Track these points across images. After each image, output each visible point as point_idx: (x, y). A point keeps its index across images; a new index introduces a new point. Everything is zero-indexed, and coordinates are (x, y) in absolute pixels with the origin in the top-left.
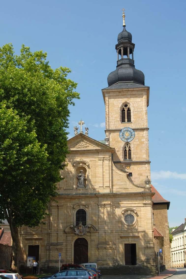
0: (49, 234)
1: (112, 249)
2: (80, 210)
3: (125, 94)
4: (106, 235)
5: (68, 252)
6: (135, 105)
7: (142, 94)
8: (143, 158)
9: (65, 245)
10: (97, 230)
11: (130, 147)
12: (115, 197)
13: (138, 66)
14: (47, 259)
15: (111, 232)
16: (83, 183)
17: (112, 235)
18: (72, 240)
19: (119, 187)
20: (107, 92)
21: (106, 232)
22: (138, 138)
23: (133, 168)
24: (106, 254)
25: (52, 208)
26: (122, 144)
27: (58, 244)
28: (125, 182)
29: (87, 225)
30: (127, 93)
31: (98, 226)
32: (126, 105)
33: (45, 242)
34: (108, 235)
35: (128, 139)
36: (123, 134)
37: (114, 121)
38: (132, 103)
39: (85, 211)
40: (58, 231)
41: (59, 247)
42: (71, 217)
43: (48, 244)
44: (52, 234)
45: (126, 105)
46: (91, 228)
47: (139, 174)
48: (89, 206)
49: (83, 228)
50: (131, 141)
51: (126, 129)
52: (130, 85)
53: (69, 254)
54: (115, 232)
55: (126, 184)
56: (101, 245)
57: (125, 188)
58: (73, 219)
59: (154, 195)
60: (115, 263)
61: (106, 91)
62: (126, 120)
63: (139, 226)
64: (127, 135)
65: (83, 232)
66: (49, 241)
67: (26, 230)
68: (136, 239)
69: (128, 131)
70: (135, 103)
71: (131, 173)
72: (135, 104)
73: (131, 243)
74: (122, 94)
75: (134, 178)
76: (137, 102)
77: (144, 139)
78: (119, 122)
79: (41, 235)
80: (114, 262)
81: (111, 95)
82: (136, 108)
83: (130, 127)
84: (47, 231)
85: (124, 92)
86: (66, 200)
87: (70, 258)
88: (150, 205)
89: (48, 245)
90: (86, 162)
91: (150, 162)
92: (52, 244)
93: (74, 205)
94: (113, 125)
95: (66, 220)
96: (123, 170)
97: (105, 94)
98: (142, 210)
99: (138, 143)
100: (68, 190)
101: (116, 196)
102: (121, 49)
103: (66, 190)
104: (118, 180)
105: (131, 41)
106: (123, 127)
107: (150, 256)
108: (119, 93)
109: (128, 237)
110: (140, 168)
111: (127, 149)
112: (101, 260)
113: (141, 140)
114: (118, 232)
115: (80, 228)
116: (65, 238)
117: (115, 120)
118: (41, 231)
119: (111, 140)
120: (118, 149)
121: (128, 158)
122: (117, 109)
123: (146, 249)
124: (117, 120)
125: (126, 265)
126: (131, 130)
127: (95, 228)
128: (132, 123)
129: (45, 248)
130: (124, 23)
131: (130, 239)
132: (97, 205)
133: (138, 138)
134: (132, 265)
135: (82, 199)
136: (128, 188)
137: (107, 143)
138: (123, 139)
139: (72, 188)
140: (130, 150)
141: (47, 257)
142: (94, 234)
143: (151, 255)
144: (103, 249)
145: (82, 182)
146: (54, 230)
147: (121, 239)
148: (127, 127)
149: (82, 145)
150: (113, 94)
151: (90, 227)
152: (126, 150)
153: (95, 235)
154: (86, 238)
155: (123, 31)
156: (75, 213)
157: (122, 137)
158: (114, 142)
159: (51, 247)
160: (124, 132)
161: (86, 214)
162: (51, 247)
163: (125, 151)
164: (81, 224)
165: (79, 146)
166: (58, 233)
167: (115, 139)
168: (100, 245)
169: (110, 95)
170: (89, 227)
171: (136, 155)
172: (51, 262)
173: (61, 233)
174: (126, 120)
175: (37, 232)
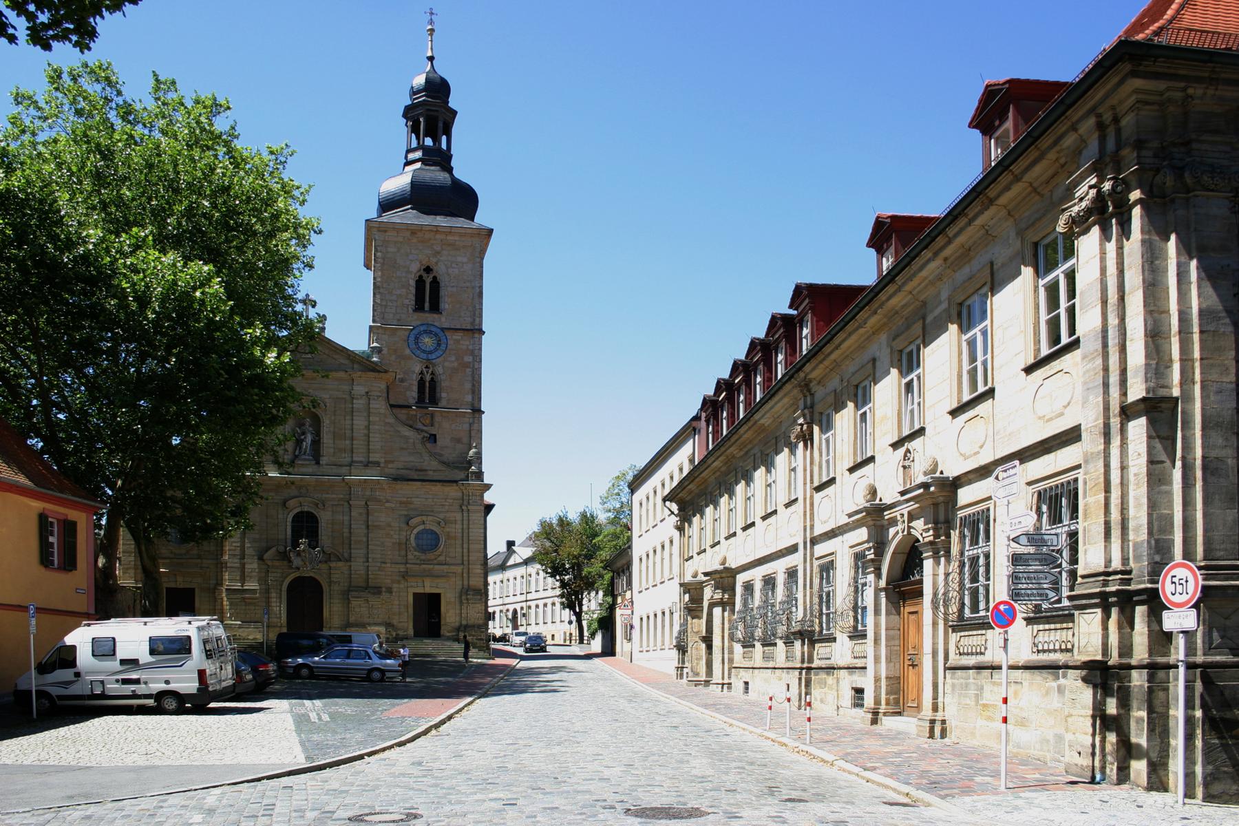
2: (302, 512)
11: (432, 373)
17: (383, 573)
35: (431, 352)
38: (446, 265)
48: (327, 506)
62: (427, 305)
69: (431, 332)
70: (454, 265)
71: (435, 435)
72: (454, 268)
77: (471, 357)
83: (435, 324)
91: (484, 412)
94: (391, 315)
99: (456, 364)
105: (448, 102)
106: (419, 323)
117: (396, 301)
120: (401, 376)
126: (438, 331)
132: (346, 504)
136: (426, 470)
154: (316, 577)
158: (393, 358)
161: (317, 522)
174: (427, 305)
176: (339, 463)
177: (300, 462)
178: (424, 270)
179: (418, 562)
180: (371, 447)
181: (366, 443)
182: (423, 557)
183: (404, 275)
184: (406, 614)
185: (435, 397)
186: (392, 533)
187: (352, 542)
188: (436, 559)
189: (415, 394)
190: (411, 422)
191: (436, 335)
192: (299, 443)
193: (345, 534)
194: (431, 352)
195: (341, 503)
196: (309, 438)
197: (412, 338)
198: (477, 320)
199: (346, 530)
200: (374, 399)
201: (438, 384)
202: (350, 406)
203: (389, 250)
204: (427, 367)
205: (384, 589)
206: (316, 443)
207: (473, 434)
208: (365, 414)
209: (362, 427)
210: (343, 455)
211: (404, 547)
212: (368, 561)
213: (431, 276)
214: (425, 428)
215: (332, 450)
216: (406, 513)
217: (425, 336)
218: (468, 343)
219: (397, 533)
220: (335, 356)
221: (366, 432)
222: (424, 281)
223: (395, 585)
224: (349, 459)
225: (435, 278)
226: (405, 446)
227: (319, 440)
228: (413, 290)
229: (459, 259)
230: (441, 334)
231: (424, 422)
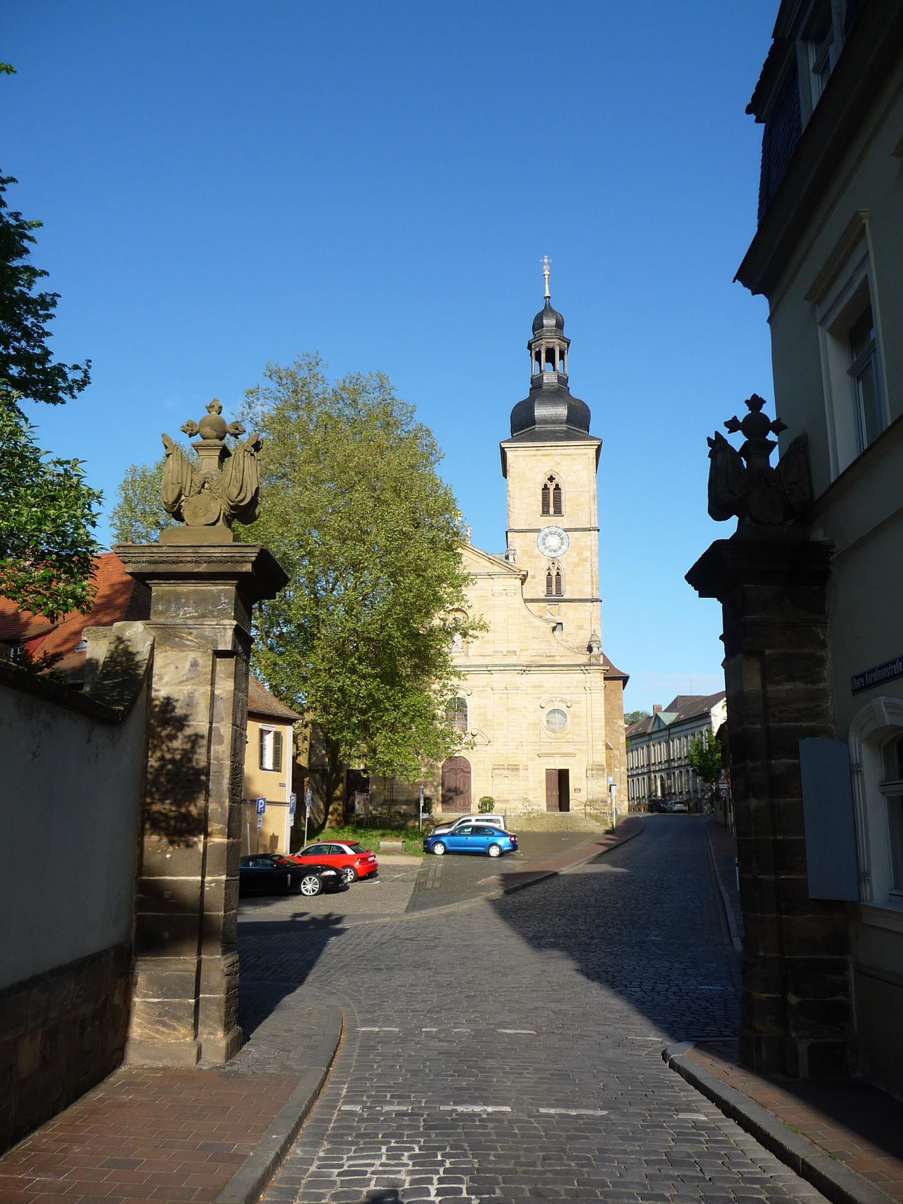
11: (558, 569)
13: (576, 391)
23: (565, 614)
26: (545, 564)
30: (554, 452)
32: (551, 476)
45: (551, 476)
48: (474, 692)
71: (561, 624)
104: (534, 638)
111: (554, 573)
121: (554, 593)
130: (547, 291)
134: (560, 811)
138: (547, 552)
140: (558, 574)
152: (549, 574)
157: (543, 547)
160: (546, 535)
168: (496, 771)
169: (517, 453)
178: (548, 479)
179: (550, 740)
182: (553, 735)
185: (560, 589)
189: (545, 588)
190: (541, 614)
201: (562, 578)
204: (553, 564)
205: (521, 767)
214: (553, 618)
216: (539, 696)
218: (586, 540)
220: (480, 560)
223: (530, 763)
225: (557, 485)
230: (564, 534)
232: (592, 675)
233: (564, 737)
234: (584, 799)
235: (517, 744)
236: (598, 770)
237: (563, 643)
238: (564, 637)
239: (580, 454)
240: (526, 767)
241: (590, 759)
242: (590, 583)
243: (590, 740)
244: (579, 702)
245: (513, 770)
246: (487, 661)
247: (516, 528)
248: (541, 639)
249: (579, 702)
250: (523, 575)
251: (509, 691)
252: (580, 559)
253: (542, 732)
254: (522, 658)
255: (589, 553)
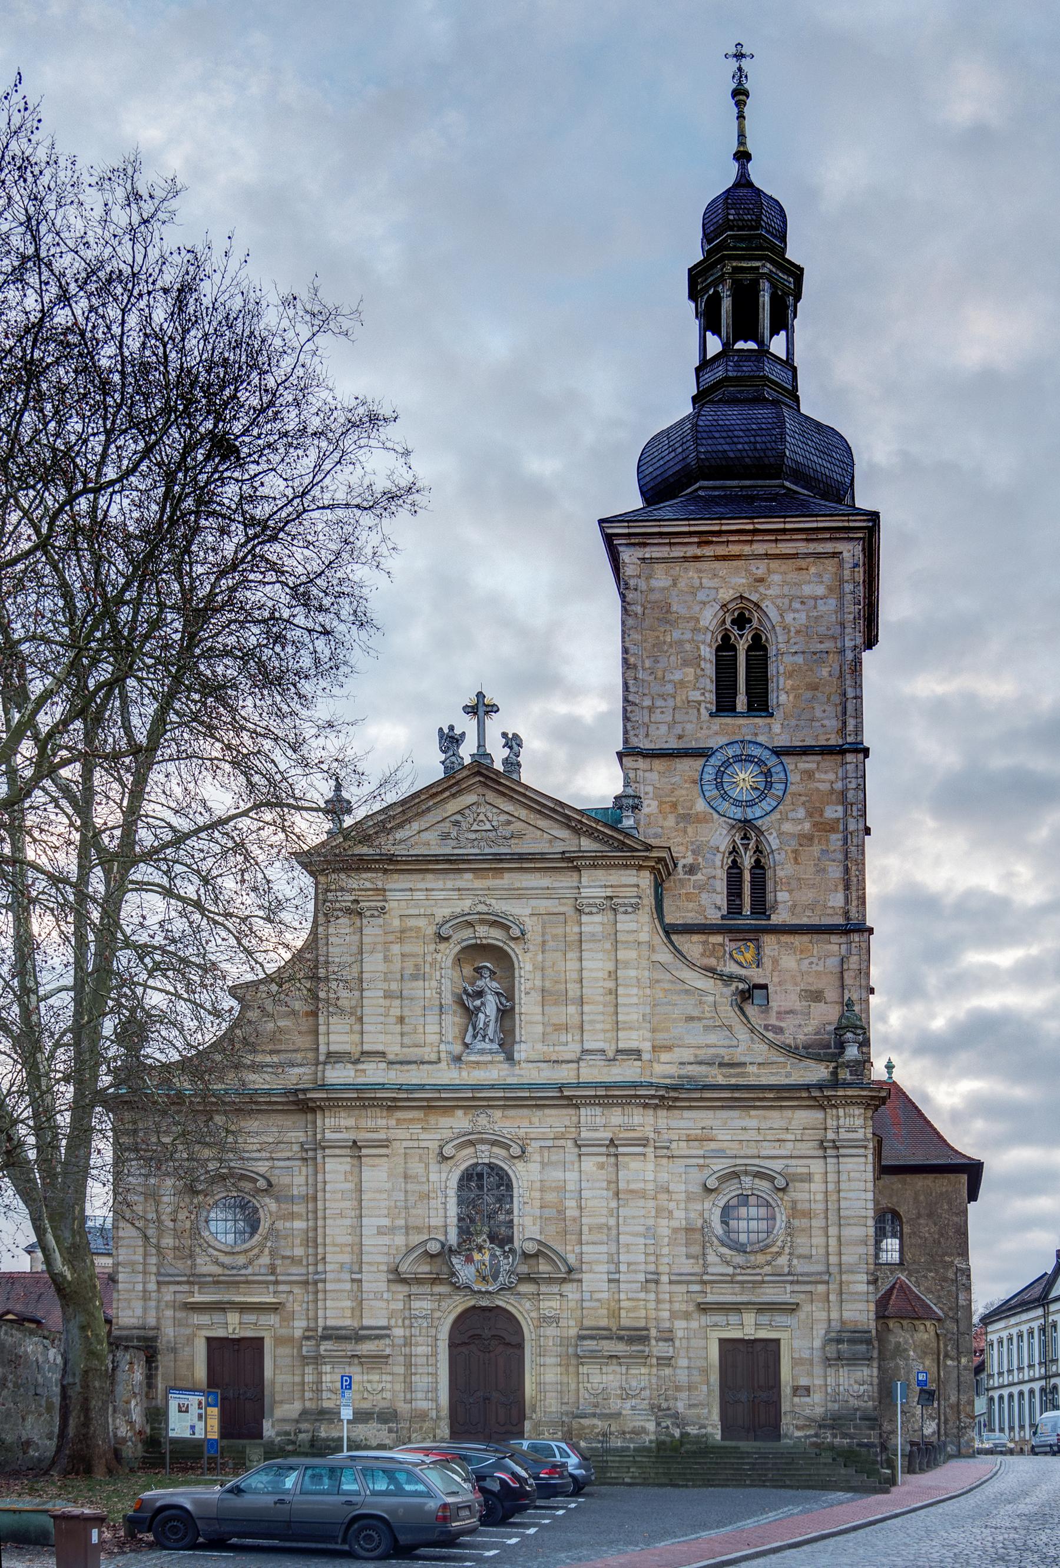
0: (316, 1283)
1: (654, 1361)
3: (734, 549)
4: (623, 1296)
5: (420, 1371)
6: (792, 615)
7: (835, 555)
8: (833, 907)
9: (401, 1341)
10: (570, 1271)
12: (670, 1108)
14: (308, 1404)
15: (647, 1281)
16: (495, 1031)
18: (437, 1314)
19: (696, 1056)
20: (629, 535)
21: (618, 1281)
22: (804, 798)
23: (775, 962)
24: (622, 1388)
25: (324, 1157)
27: (362, 1332)
28: (729, 1028)
29: (516, 1244)
30: (747, 549)
31: (577, 1249)
33: (297, 1324)
34: (630, 1295)
35: (751, 803)
36: (720, 774)
37: (671, 703)
39: (507, 1175)
40: (360, 1272)
41: (367, 1348)
42: (433, 1202)
43: (311, 1334)
44: (329, 1286)
45: (741, 615)
46: (541, 1260)
47: (806, 991)
48: (529, 1149)
49: (493, 1256)
50: (767, 818)
51: (735, 750)
52: (766, 500)
53: (421, 1381)
54: (671, 1282)
55: (735, 1043)
56: (595, 1343)
57: (726, 1060)
58: (441, 1212)
59: (883, 1100)
60: (667, 1427)
61: (626, 531)
63: (799, 1257)
64: (745, 778)
65: (495, 1277)
66: (316, 1319)
67: (189, 1262)
68: (780, 1319)
72: (798, 611)
73: (752, 1338)
74: (721, 550)
75: (778, 1013)
76: (802, 603)
78: (699, 710)
79: (271, 1288)
80: (664, 1424)
81: (654, 555)
82: (798, 632)
84: (303, 1271)
85: (731, 538)
86: (400, 1114)
87: (427, 1399)
88: (862, 1151)
89: (308, 1338)
90: (511, 918)
91: (871, 931)
92: (332, 1334)
93: (447, 1143)
94: (664, 729)
95: (403, 1215)
96: (719, 969)
97: (621, 549)
98: (818, 1178)
100: (414, 1067)
101: (676, 1099)
102: (716, 293)
103: (398, 1066)
104: (690, 1019)
106: (724, 740)
107: (851, 1399)
108: (700, 544)
109: (736, 1308)
110: (815, 960)
112: (594, 1415)
113: (821, 815)
114: (688, 1283)
115: (477, 1256)
116: (400, 1305)
118: (273, 1269)
119: (649, 807)
121: (747, 910)
122: (688, 636)
123: (830, 1366)
124: (689, 702)
125: (722, 1439)
126: (766, 754)
127: (565, 1261)
128: (772, 715)
129: (295, 1351)
131: (749, 1318)
132: (570, 1143)
133: (804, 798)
135: (489, 1111)
136: (744, 1064)
137: (628, 822)
139: (433, 1057)
141: (308, 1395)
142: (555, 1289)
143: (858, 1397)
144: (607, 1364)
145: (492, 1024)
146: (342, 1264)
147: (703, 1318)
148: (742, 742)
149: (488, 827)
150: (667, 548)
151: (536, 1255)
153: (561, 1295)
155: (737, 185)
156: (453, 1183)
157: (715, 792)
158: (671, 821)
159: (322, 1348)
160: (727, 764)
162: (326, 1346)
163: (730, 868)
164: (485, 1237)
165: (473, 836)
166: (360, 1281)
167: (674, 805)
168: (585, 1343)
170: (526, 1256)
171: (790, 891)
172: (327, 1417)
173: (375, 1281)
175: (250, 1271)
176: (554, 1058)
177: (473, 1058)
178: (733, 622)
179: (730, 1270)
180: (621, 1018)
181: (612, 1009)
182: (739, 1259)
183: (688, 636)
184: (705, 1388)
185: (763, 902)
186: (672, 1205)
187: (585, 1229)
188: (769, 1263)
189: (722, 900)
190: (712, 962)
191: (760, 763)
192: (471, 1014)
193: (569, 1213)
194: (751, 803)
195: (561, 1142)
196: (491, 1006)
197: (710, 774)
198: (851, 723)
199: (571, 1203)
200: (626, 912)
201: (769, 873)
202: (576, 929)
203: (654, 583)
205: (653, 1333)
206: (506, 1014)
207: (848, 981)
208: (608, 946)
209: (600, 975)
210: (563, 1038)
211: (698, 1236)
212: (619, 1272)
213: (748, 635)
215: (540, 1029)
216: (701, 1161)
217: (736, 767)
219: (683, 1206)
221: (611, 985)
222: (734, 648)
223: (680, 1324)
224: (577, 1048)
225: (757, 638)
226: (695, 1014)
227: (513, 1008)
228: (710, 669)
229: (807, 590)
230: (772, 761)
231: (740, 958)
232: (841, 1112)
233: (769, 1263)
234: (819, 1411)
235: (641, 1277)
236: (852, 1341)
237: (770, 1035)
238: (773, 1021)
239: (818, 556)
240: (666, 1335)
241: (834, 1315)
242: (841, 887)
243: (834, 1270)
244: (808, 1178)
245: (631, 1340)
246: (565, 1074)
247: (645, 744)
248: (710, 1023)
249: (808, 1178)
250: (660, 860)
251: (621, 1150)
252: (815, 825)
253: (709, 1251)
254: (658, 1069)
255: (840, 808)
